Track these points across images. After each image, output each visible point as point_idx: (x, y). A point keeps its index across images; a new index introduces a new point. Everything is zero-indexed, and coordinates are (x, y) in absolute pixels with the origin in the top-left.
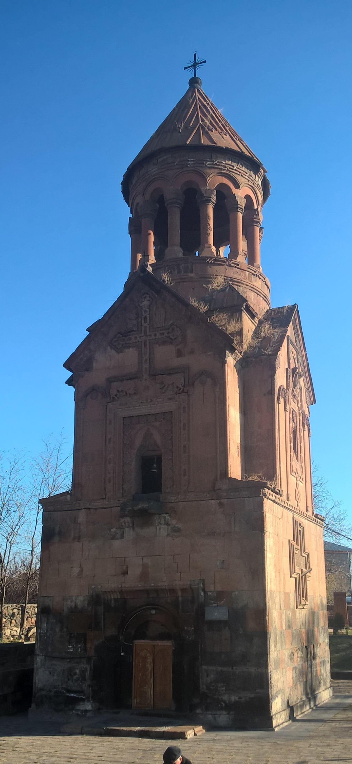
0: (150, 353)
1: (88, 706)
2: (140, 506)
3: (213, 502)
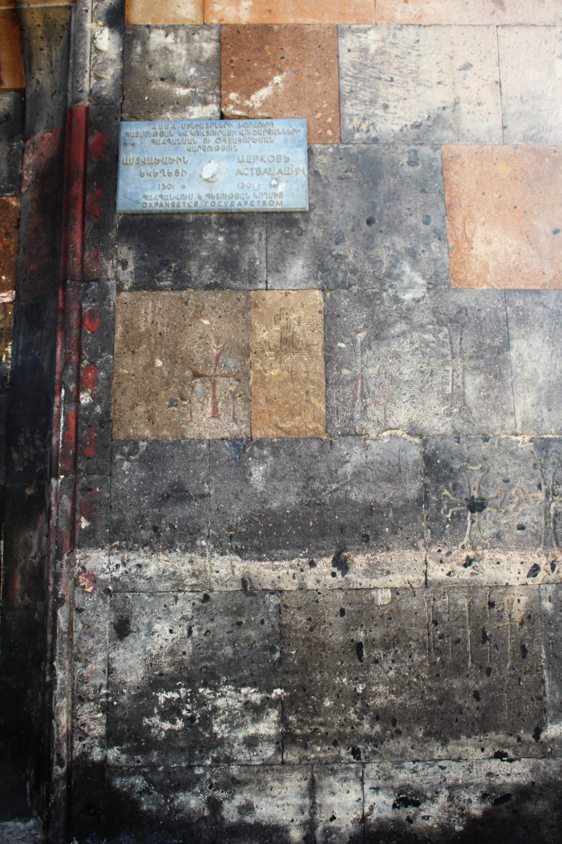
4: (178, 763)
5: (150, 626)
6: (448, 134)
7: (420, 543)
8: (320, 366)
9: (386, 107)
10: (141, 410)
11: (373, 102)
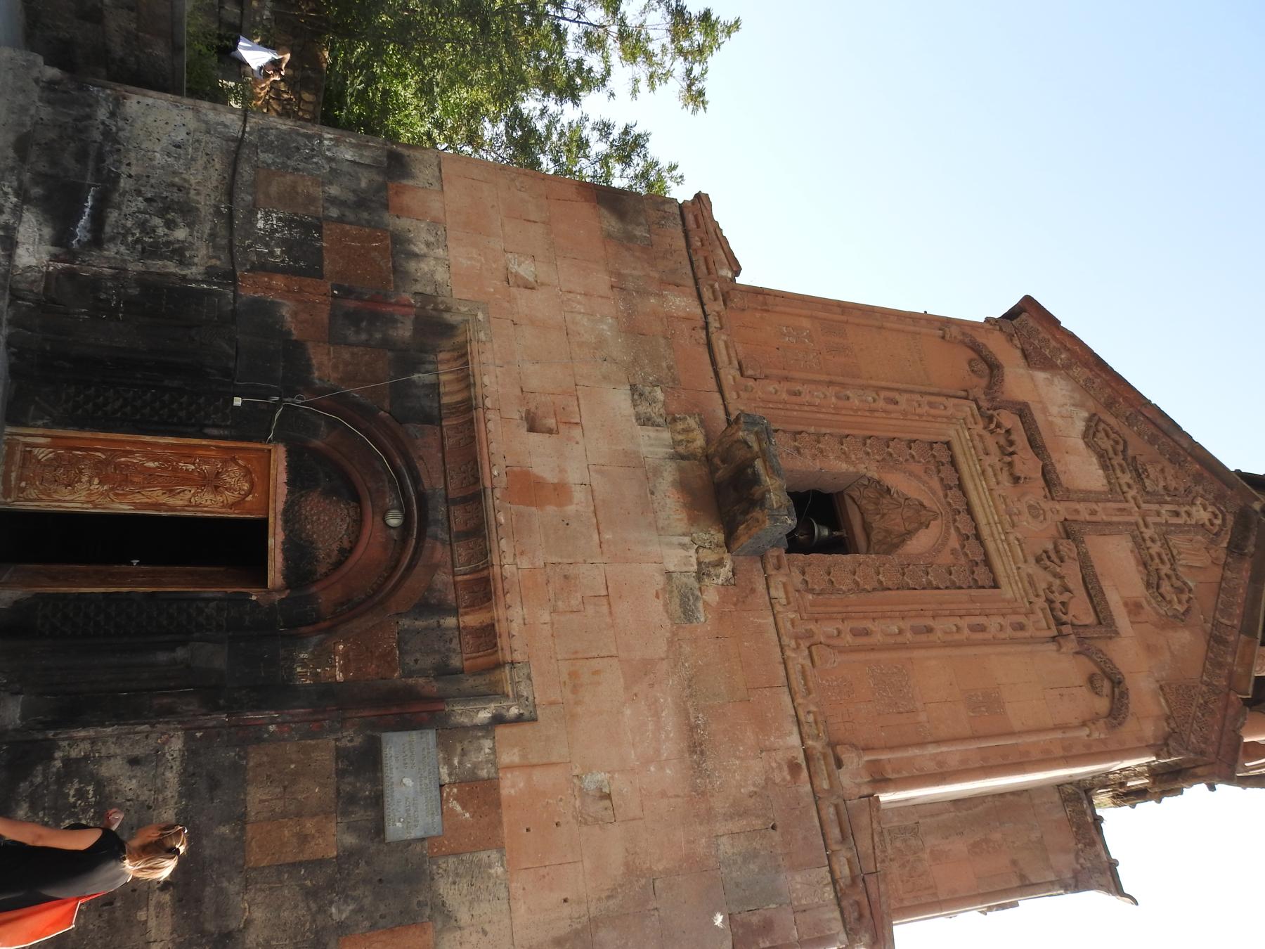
0: (1111, 523)
2: (768, 481)
3: (794, 740)
4: (47, 802)
5: (135, 777)
6: (439, 925)
7: (175, 936)
8: (289, 860)
9: (454, 883)
10: (265, 759)
11: (457, 875)
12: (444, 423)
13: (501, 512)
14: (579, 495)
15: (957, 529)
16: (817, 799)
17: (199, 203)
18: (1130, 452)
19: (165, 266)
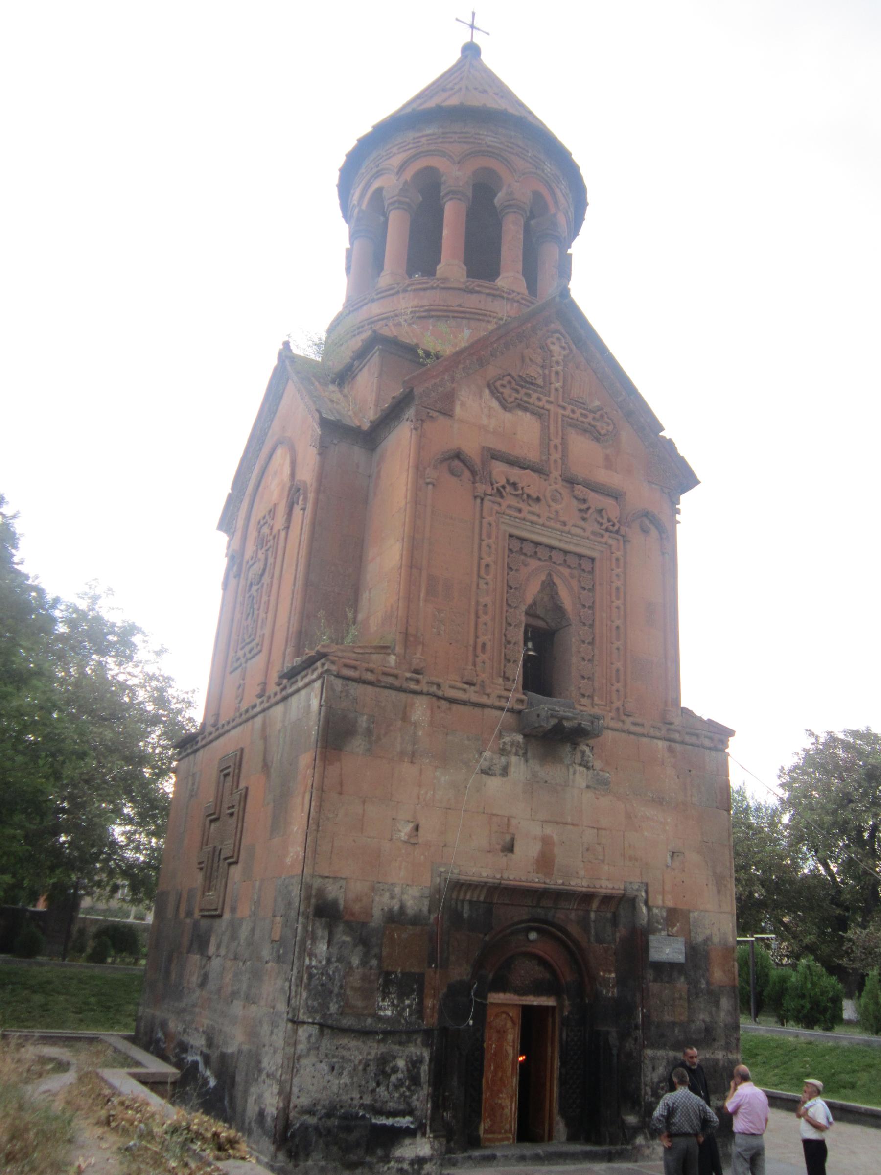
1: (423, 1147)
3: (660, 744)
12: (495, 901)
13: (556, 882)
14: (549, 830)
15: (560, 565)
16: (683, 743)
17: (377, 1053)
18: (514, 374)
19: (425, 1071)
